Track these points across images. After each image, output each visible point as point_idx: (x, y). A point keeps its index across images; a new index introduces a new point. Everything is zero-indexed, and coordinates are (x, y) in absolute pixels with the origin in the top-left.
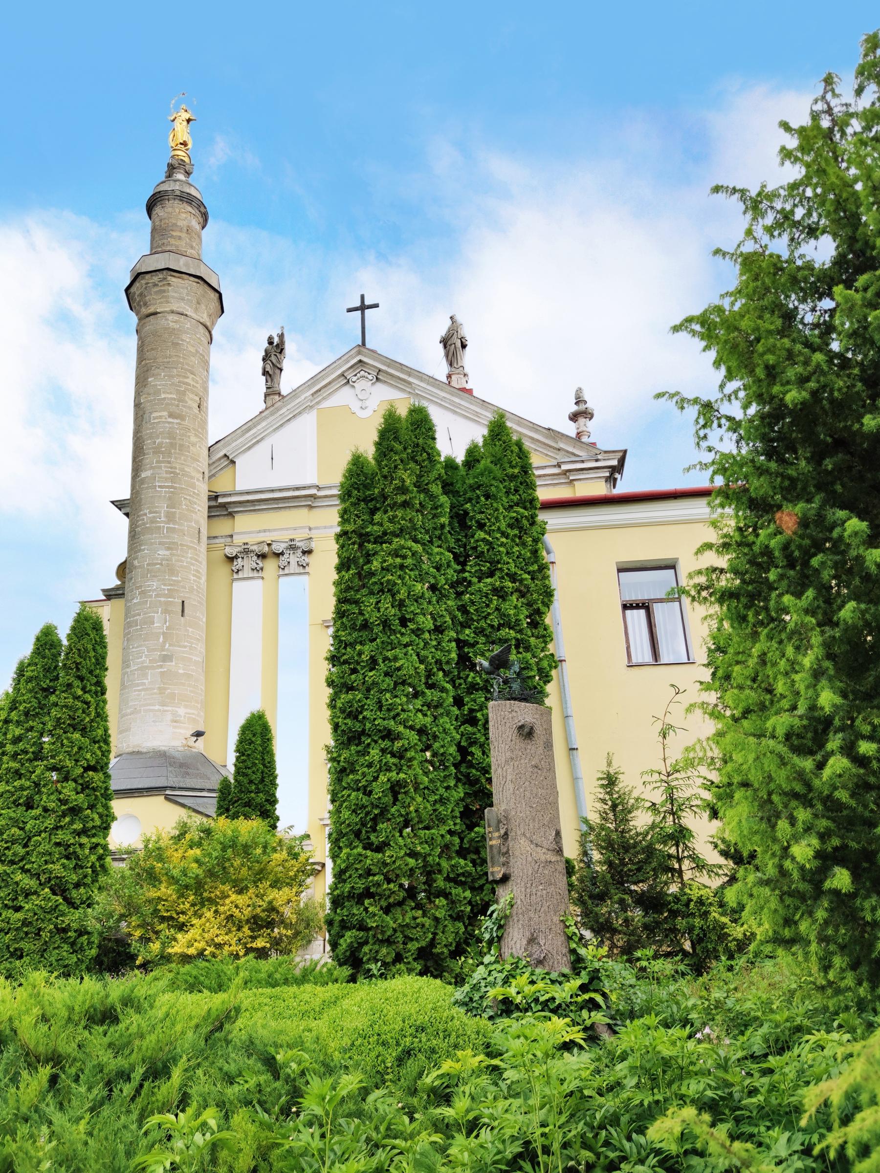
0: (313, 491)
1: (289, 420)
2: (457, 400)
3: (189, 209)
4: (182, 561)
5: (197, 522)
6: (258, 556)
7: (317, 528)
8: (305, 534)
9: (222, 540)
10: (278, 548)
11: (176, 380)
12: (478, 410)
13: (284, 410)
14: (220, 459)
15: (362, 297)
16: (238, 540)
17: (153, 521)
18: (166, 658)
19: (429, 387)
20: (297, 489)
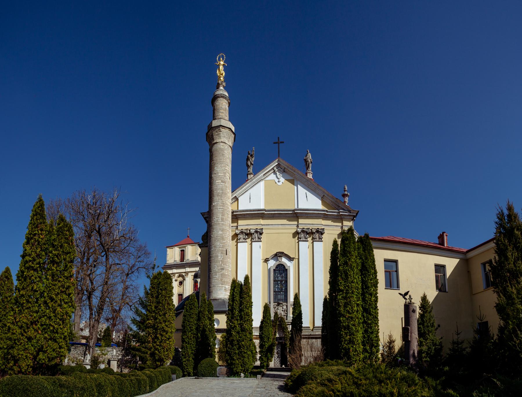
3: (225, 101)
11: (223, 168)
17: (217, 221)
18: (223, 269)
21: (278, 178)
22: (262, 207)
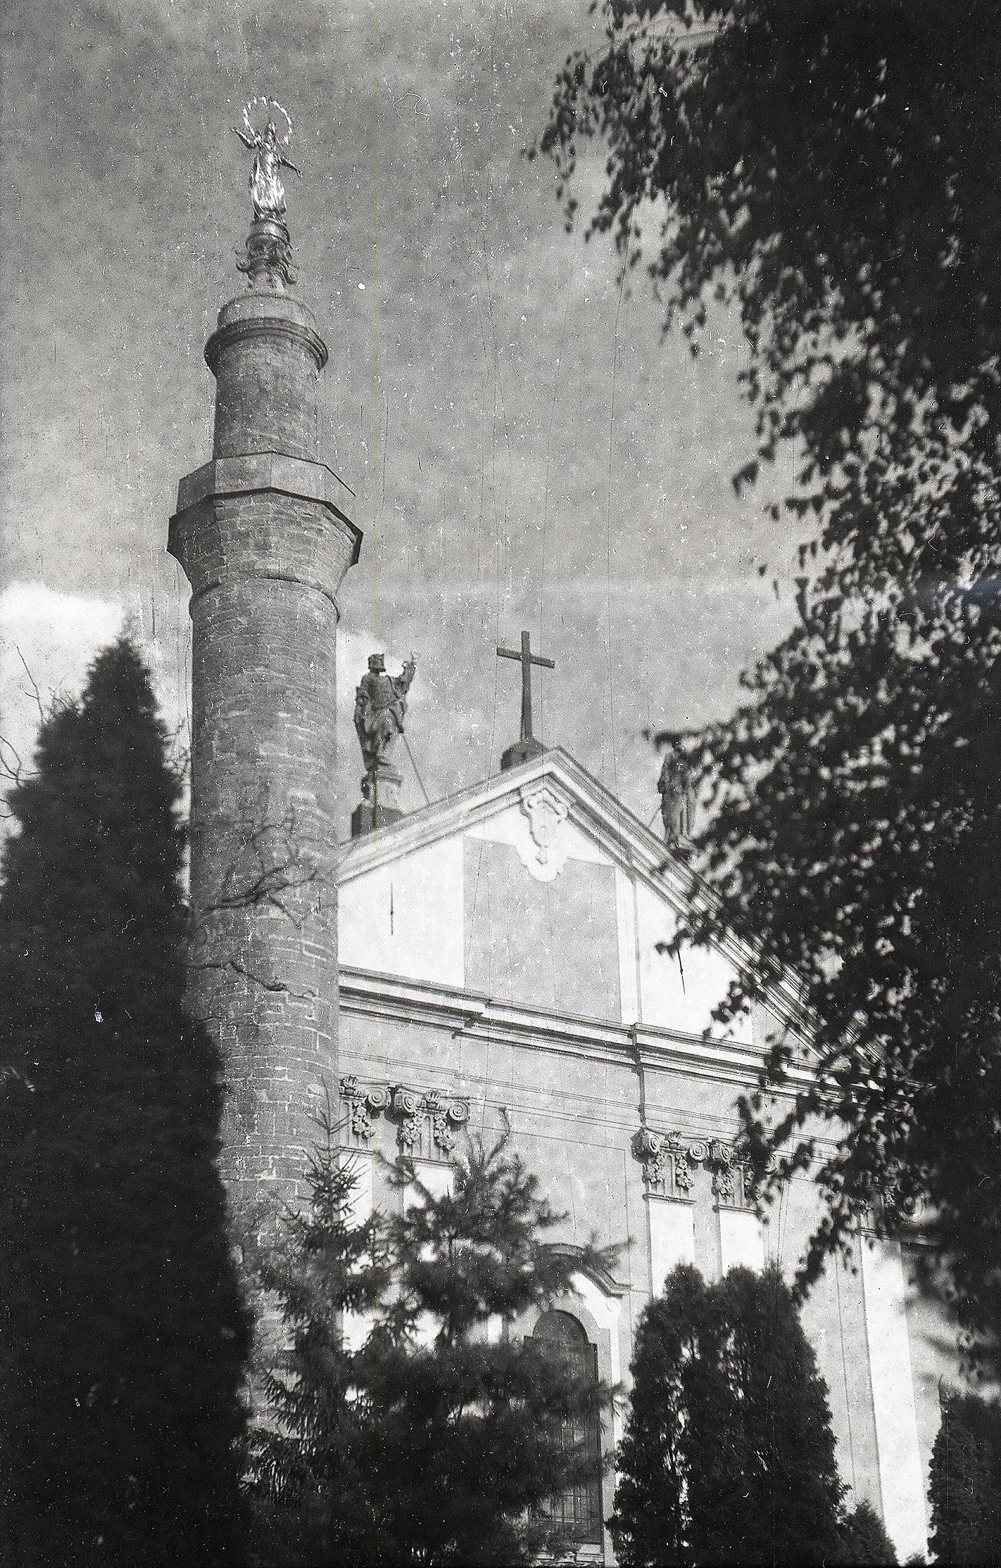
6: (368, 1105)
10: (413, 1102)
20: (454, 994)
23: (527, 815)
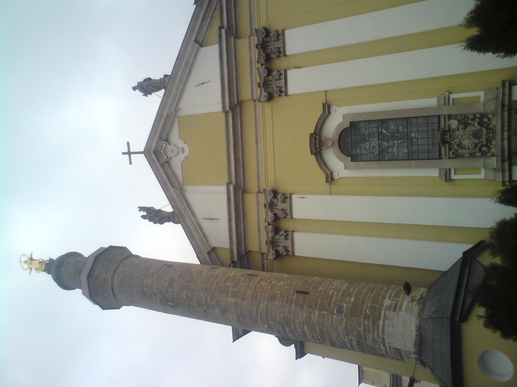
0: (231, 187)
1: (188, 205)
2: (178, 79)
4: (267, 290)
5: (242, 276)
7: (259, 188)
8: (262, 196)
9: (265, 261)
12: (184, 63)
13: (180, 207)
14: (210, 258)
15: (124, 153)
16: (265, 248)
19: (169, 102)
21: (178, 152)
22: (224, 188)
23: (170, 158)
